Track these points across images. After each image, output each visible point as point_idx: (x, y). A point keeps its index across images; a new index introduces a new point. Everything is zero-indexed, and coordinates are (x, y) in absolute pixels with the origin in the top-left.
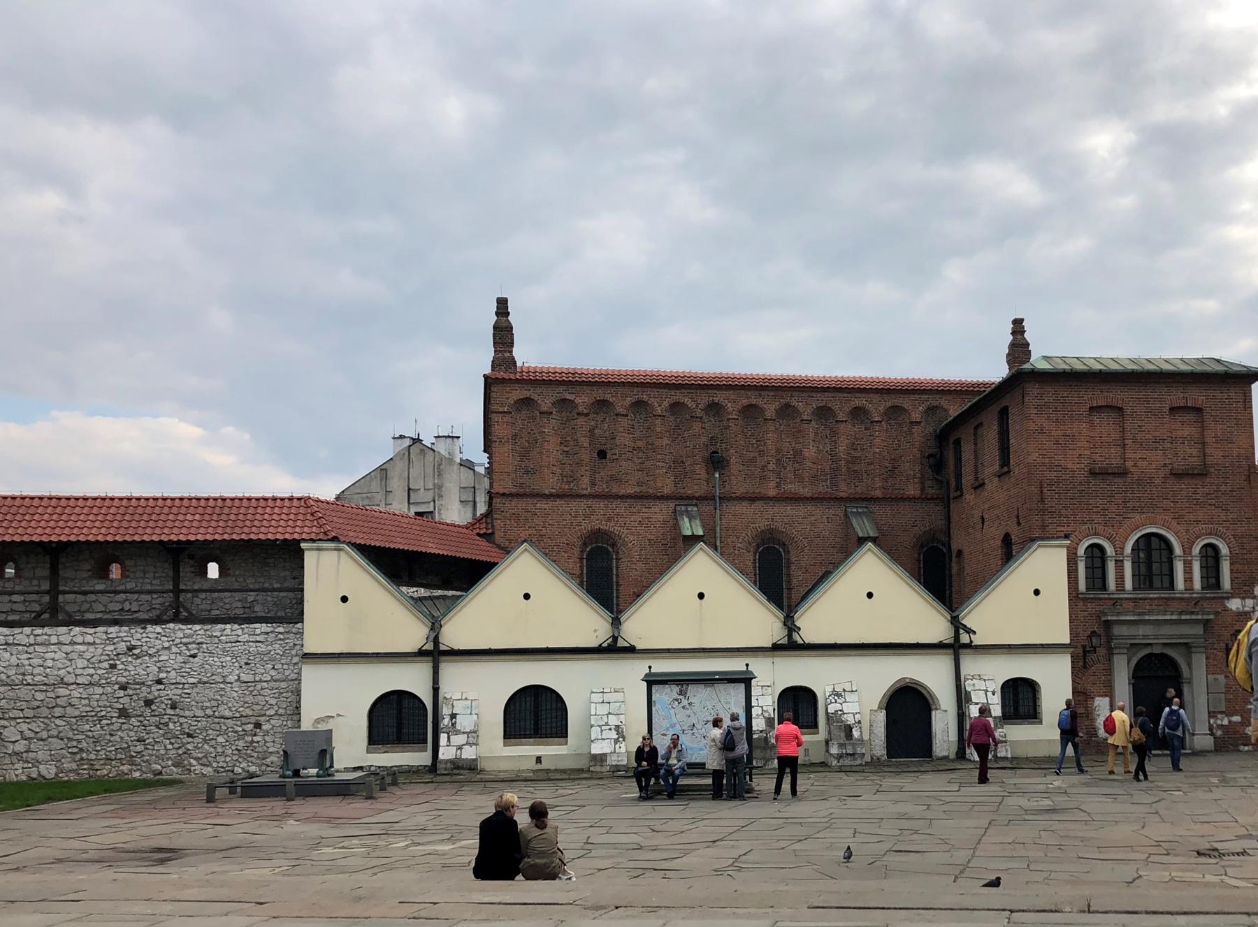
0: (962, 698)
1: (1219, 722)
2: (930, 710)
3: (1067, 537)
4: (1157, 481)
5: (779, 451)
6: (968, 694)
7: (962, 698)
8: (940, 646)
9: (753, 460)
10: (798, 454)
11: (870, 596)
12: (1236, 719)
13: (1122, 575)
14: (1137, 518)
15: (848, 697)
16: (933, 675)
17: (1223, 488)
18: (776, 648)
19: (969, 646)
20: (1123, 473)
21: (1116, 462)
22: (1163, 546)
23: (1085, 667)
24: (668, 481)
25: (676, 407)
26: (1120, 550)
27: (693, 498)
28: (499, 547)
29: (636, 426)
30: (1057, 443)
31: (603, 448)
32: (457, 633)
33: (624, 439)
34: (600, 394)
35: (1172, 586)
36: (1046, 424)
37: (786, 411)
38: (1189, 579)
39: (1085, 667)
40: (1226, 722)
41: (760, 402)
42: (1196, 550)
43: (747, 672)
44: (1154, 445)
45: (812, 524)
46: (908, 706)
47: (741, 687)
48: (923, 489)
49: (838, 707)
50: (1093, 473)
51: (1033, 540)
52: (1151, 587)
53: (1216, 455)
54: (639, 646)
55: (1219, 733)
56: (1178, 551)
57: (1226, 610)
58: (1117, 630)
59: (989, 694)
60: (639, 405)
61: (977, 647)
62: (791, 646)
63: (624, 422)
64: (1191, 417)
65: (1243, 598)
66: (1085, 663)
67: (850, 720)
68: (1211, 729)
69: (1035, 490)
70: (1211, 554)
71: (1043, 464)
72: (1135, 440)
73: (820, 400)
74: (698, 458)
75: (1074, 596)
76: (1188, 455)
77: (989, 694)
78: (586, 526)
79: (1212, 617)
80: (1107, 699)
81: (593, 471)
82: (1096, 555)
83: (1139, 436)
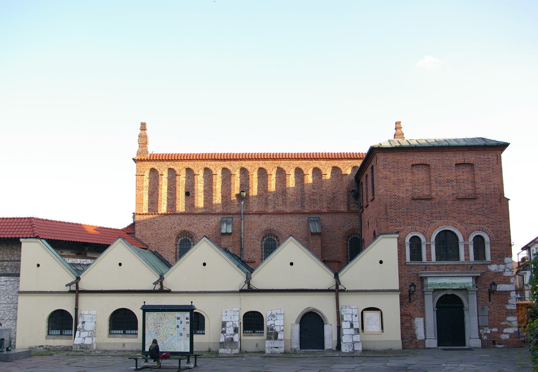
0: (339, 319)
1: (485, 332)
3: (397, 233)
6: (342, 316)
7: (339, 319)
11: (293, 264)
12: (495, 330)
13: (430, 252)
15: (280, 317)
16: (324, 306)
17: (485, 206)
18: (242, 291)
19: (343, 291)
20: (429, 199)
21: (426, 193)
23: (410, 302)
26: (428, 239)
27: (230, 214)
28: (137, 239)
30: (394, 184)
32: (87, 281)
36: (388, 173)
38: (467, 255)
40: (489, 332)
43: (192, 305)
45: (291, 226)
46: (311, 323)
47: (188, 314)
49: (272, 322)
51: (381, 234)
54: (172, 290)
55: (485, 338)
56: (461, 239)
57: (489, 271)
59: (354, 316)
61: (348, 291)
64: (468, 169)
65: (499, 264)
66: (410, 299)
67: (277, 329)
69: (382, 208)
70: (479, 242)
75: (402, 263)
76: (467, 189)
77: (354, 316)
78: (179, 229)
79: (479, 275)
80: (422, 319)
82: (415, 241)
83: (438, 180)
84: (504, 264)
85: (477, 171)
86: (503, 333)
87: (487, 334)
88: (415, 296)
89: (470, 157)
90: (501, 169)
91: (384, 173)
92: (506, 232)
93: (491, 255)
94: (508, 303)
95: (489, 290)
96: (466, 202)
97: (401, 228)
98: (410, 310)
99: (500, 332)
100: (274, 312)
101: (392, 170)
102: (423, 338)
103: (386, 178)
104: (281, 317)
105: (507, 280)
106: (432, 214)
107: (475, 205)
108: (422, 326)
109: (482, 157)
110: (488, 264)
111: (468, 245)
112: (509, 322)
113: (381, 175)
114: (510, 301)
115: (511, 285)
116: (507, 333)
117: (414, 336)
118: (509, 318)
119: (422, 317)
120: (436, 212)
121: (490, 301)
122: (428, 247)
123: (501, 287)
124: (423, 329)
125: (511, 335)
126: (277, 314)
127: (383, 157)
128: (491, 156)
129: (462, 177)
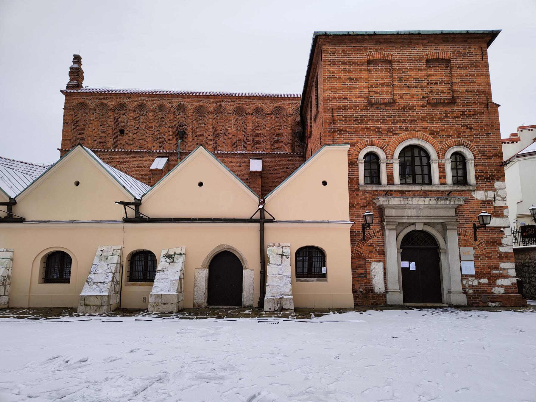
1: (470, 283)
2: (242, 270)
4: (418, 109)
5: (215, 130)
8: (251, 221)
9: (202, 135)
10: (226, 131)
12: (484, 281)
14: (403, 134)
20: (392, 103)
21: (387, 97)
22: (423, 154)
24: (155, 145)
25: (161, 107)
26: (390, 157)
29: (141, 117)
30: (344, 84)
31: (123, 128)
33: (132, 123)
34: (121, 100)
35: (430, 182)
37: (219, 110)
38: (443, 177)
39: (364, 239)
40: (476, 283)
41: (206, 104)
42: (448, 155)
44: (417, 84)
48: (293, 150)
50: (370, 103)
52: (414, 182)
53: (461, 90)
55: (471, 291)
57: (473, 199)
58: (387, 212)
60: (142, 106)
62: (139, 219)
63: (132, 114)
64: (443, 67)
65: (486, 191)
66: (364, 236)
68: (464, 288)
70: (459, 160)
71: (334, 98)
72: (400, 81)
73: (238, 103)
74: (171, 133)
79: (462, 203)
80: (381, 264)
81: (115, 140)
84: (494, 190)
85: (455, 68)
86: (495, 285)
87: (473, 286)
88: (371, 232)
89: (447, 51)
90: (487, 66)
91: (332, 70)
92: (495, 148)
93: (477, 178)
94: (501, 244)
95: (474, 225)
96: (440, 108)
98: (365, 250)
99: (492, 284)
100: (171, 252)
101: (342, 67)
102: (383, 290)
103: (334, 76)
104: (182, 258)
105: (499, 212)
106: (394, 123)
107: (452, 111)
108: (382, 274)
109: (462, 50)
110: (471, 190)
112: (504, 269)
113: (327, 73)
114: (503, 241)
115: (504, 219)
116: (502, 286)
117: (370, 288)
118: (503, 265)
119: (380, 261)
120: (400, 120)
121: (476, 240)
122: (389, 166)
123: (495, 222)
124: (382, 278)
125: (506, 288)
126: (175, 253)
127: (330, 50)
128: (474, 50)
129: (434, 77)
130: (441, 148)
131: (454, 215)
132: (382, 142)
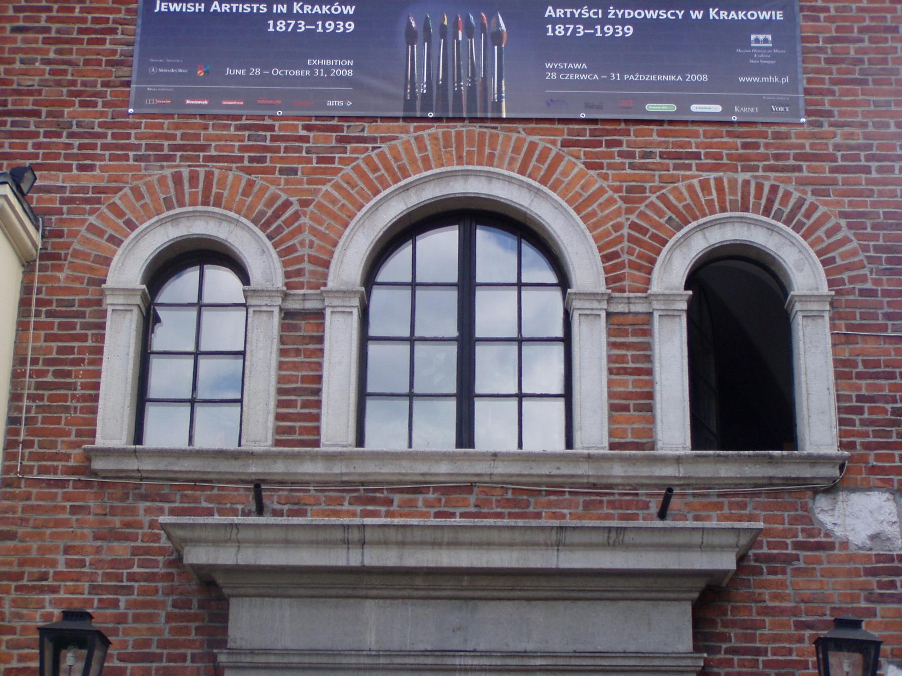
79: (727, 562)
97: (88, 180)
111: (643, 326)
130: (633, 226)
131: (686, 644)
132: (277, 188)
